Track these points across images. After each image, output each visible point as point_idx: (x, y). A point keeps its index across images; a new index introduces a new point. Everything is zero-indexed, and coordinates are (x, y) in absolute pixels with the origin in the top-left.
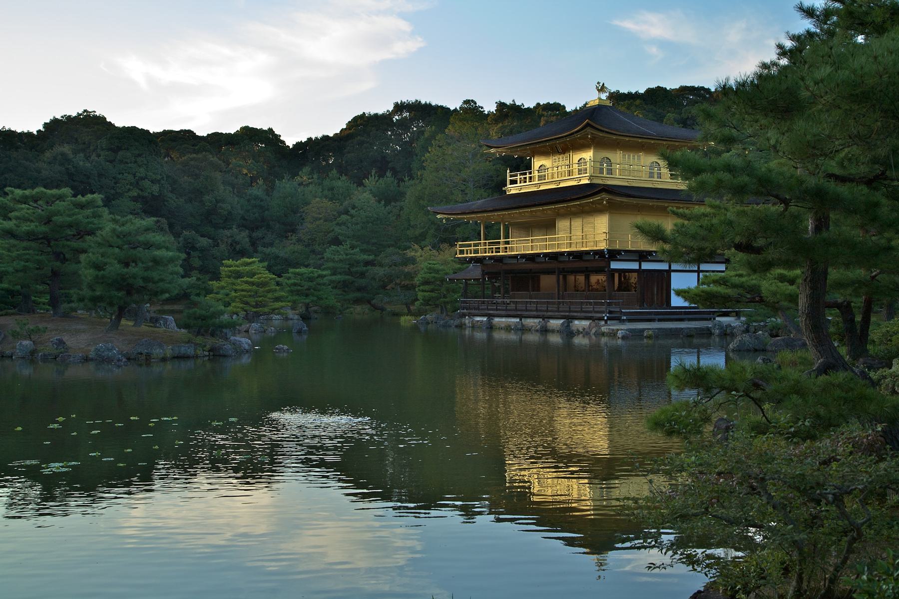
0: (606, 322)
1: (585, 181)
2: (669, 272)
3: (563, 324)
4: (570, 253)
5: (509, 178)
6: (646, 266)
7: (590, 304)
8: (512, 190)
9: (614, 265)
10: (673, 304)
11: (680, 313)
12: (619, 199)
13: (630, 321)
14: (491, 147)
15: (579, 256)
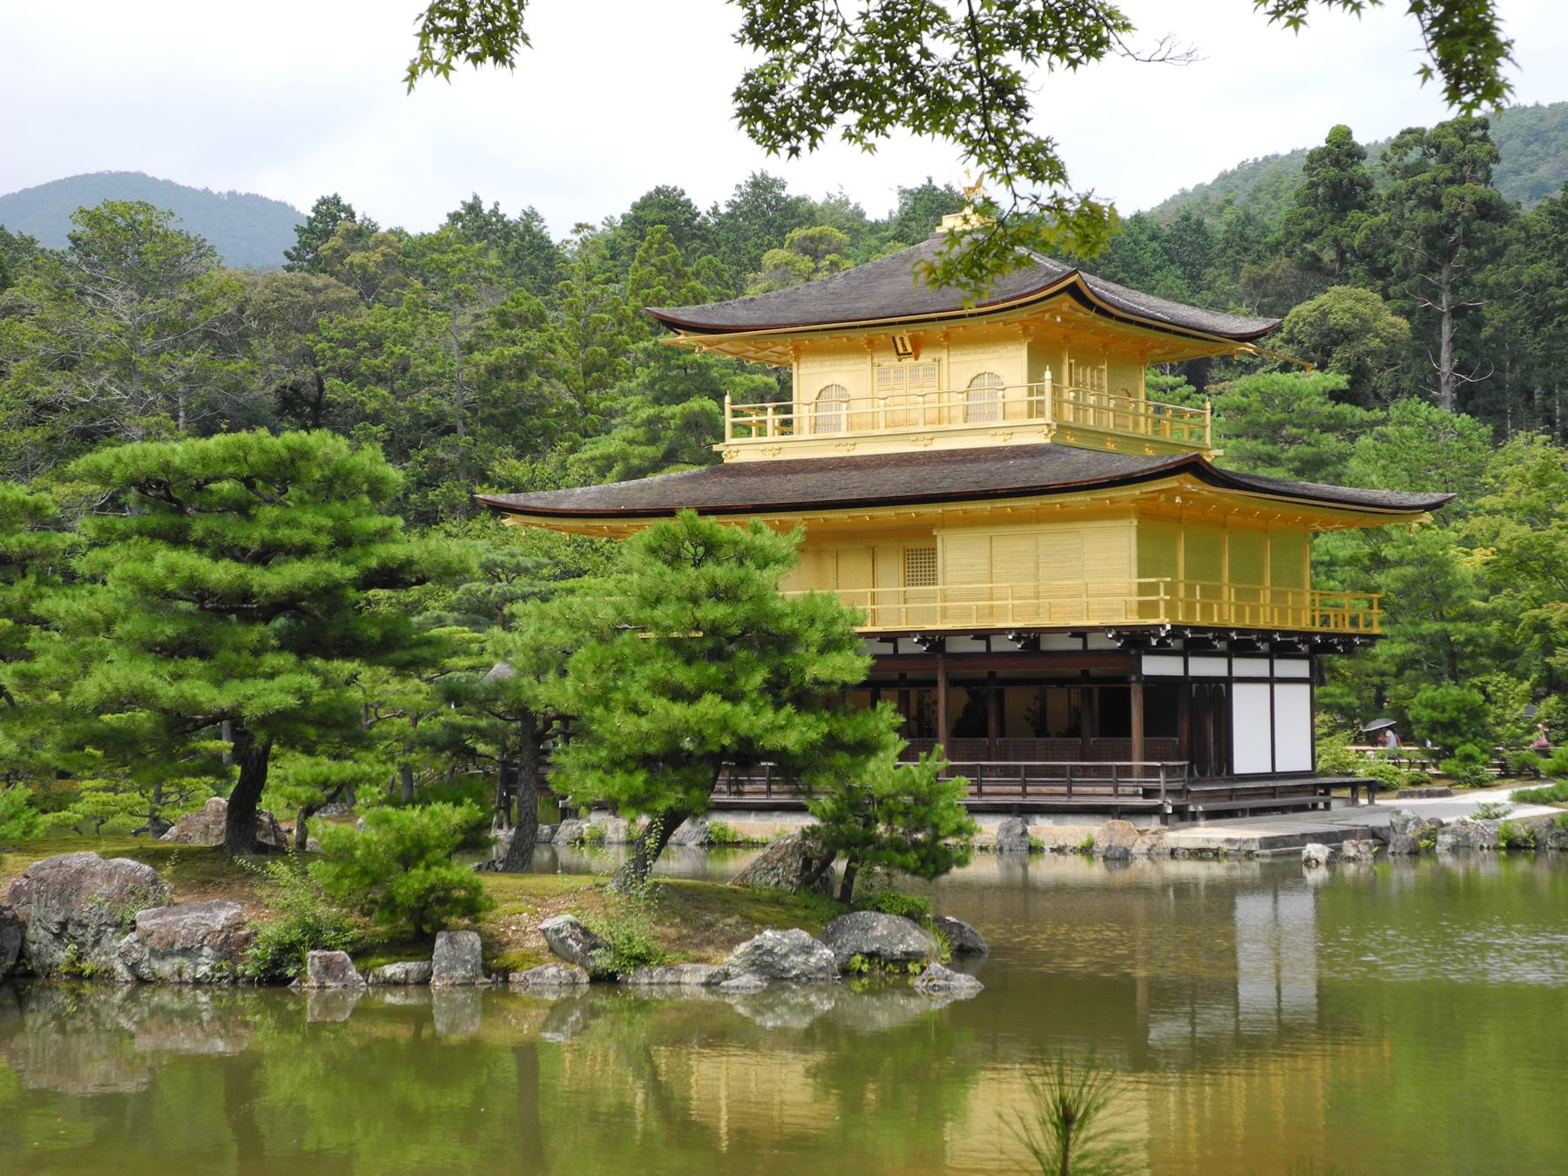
0: (1165, 819)
1: (1040, 438)
2: (1229, 680)
3: (1008, 830)
4: (1020, 634)
5: (729, 420)
6: (1204, 667)
7: (1006, 772)
8: (739, 451)
9: (1153, 666)
10: (1240, 767)
11: (1273, 793)
12: (1206, 490)
13: (1212, 815)
14: (673, 325)
15: (1030, 638)
